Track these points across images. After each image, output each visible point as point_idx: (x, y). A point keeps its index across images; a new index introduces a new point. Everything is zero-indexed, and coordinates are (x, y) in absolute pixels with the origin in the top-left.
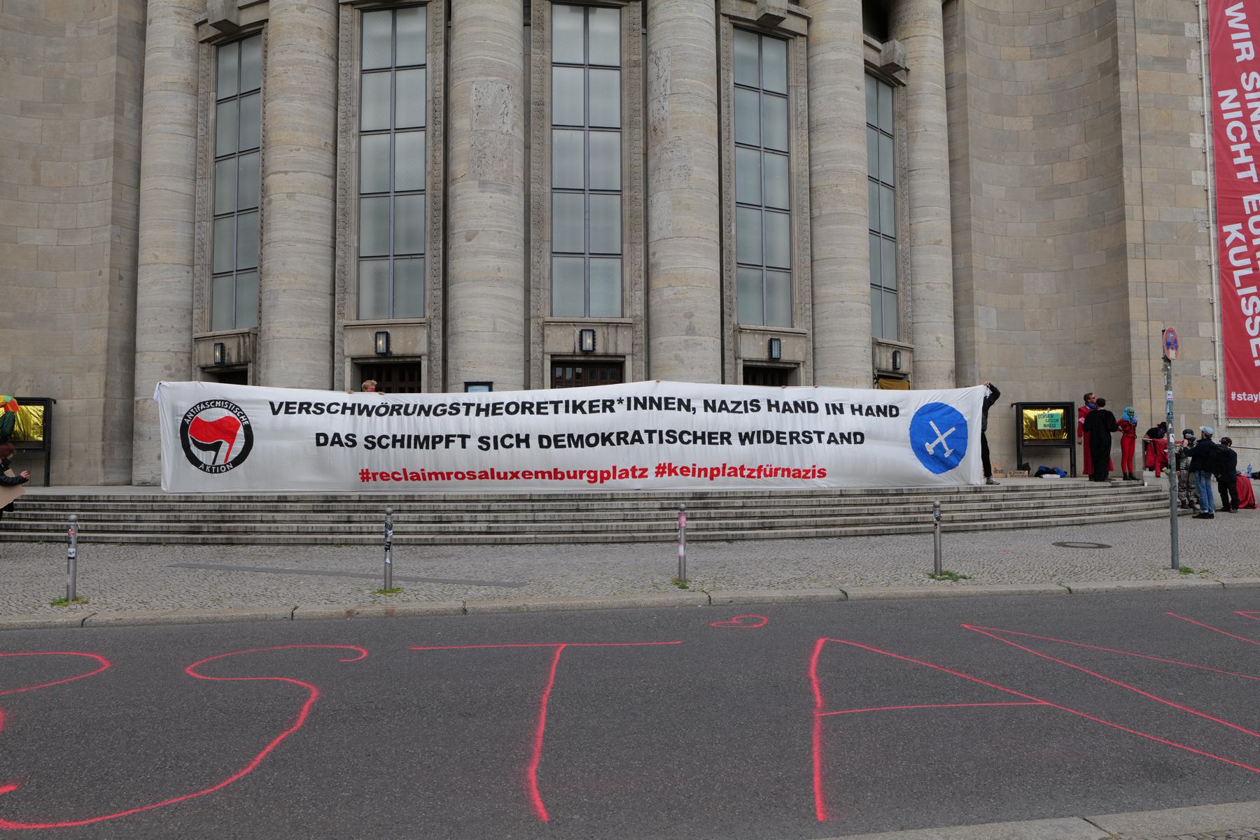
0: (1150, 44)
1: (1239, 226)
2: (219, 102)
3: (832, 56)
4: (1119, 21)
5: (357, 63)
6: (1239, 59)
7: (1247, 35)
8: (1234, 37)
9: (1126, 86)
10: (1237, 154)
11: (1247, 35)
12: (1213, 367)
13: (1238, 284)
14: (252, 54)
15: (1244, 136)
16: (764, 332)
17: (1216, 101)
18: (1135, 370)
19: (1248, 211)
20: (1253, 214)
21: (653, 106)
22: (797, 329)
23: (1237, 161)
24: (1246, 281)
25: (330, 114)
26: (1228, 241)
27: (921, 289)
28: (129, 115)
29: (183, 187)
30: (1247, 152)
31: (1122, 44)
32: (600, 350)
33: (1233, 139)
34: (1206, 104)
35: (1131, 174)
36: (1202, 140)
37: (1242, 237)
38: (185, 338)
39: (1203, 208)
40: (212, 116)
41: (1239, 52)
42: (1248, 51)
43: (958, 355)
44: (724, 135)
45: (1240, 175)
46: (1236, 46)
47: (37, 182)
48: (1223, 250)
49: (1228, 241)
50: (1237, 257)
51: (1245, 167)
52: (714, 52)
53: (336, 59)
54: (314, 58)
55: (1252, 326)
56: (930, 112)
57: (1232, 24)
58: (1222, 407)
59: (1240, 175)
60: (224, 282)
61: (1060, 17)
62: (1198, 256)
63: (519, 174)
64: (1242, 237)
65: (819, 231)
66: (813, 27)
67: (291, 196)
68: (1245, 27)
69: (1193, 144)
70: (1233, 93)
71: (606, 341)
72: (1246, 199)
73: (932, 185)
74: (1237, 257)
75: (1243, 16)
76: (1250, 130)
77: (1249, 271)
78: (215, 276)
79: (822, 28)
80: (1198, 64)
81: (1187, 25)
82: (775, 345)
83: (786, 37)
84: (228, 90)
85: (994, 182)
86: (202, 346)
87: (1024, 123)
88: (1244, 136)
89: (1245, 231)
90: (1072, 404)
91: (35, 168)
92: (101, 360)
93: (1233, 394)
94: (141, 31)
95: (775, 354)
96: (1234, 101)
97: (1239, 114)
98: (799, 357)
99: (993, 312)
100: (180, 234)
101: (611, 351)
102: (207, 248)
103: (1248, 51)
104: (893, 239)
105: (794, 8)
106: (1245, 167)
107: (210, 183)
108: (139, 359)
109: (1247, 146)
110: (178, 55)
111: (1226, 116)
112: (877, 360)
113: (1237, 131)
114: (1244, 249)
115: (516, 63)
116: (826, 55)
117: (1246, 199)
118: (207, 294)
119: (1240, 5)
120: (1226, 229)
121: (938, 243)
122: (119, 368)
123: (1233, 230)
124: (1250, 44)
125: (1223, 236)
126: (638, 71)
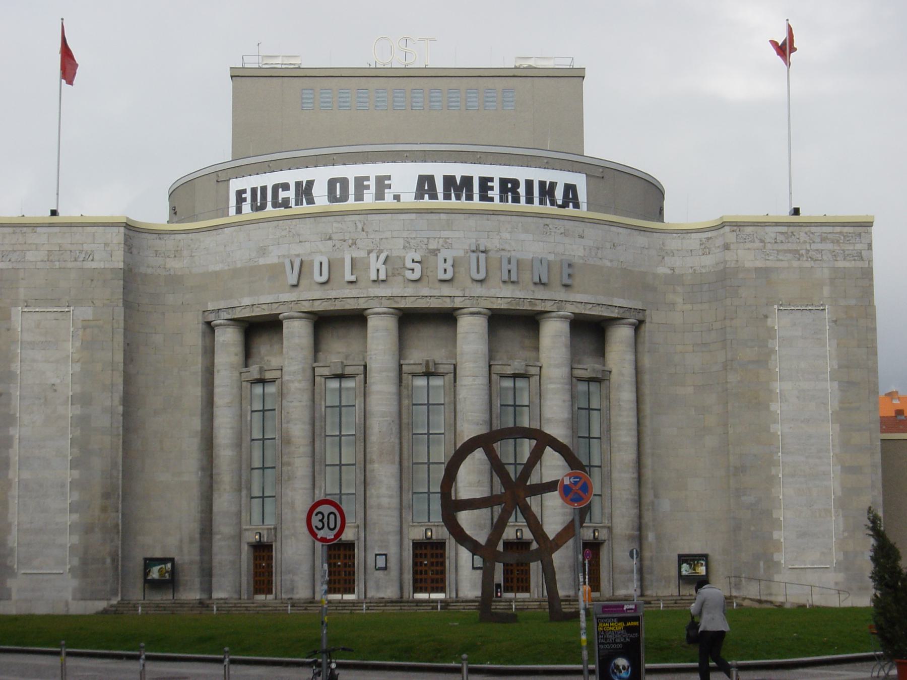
2: (252, 411)
5: (323, 403)
14: (271, 389)
32: (434, 537)
53: (313, 400)
62: (773, 472)
63: (397, 459)
66: (543, 370)
71: (437, 532)
84: (258, 406)
87: (690, 390)
90: (680, 556)
94: (209, 372)
101: (440, 537)
115: (394, 408)
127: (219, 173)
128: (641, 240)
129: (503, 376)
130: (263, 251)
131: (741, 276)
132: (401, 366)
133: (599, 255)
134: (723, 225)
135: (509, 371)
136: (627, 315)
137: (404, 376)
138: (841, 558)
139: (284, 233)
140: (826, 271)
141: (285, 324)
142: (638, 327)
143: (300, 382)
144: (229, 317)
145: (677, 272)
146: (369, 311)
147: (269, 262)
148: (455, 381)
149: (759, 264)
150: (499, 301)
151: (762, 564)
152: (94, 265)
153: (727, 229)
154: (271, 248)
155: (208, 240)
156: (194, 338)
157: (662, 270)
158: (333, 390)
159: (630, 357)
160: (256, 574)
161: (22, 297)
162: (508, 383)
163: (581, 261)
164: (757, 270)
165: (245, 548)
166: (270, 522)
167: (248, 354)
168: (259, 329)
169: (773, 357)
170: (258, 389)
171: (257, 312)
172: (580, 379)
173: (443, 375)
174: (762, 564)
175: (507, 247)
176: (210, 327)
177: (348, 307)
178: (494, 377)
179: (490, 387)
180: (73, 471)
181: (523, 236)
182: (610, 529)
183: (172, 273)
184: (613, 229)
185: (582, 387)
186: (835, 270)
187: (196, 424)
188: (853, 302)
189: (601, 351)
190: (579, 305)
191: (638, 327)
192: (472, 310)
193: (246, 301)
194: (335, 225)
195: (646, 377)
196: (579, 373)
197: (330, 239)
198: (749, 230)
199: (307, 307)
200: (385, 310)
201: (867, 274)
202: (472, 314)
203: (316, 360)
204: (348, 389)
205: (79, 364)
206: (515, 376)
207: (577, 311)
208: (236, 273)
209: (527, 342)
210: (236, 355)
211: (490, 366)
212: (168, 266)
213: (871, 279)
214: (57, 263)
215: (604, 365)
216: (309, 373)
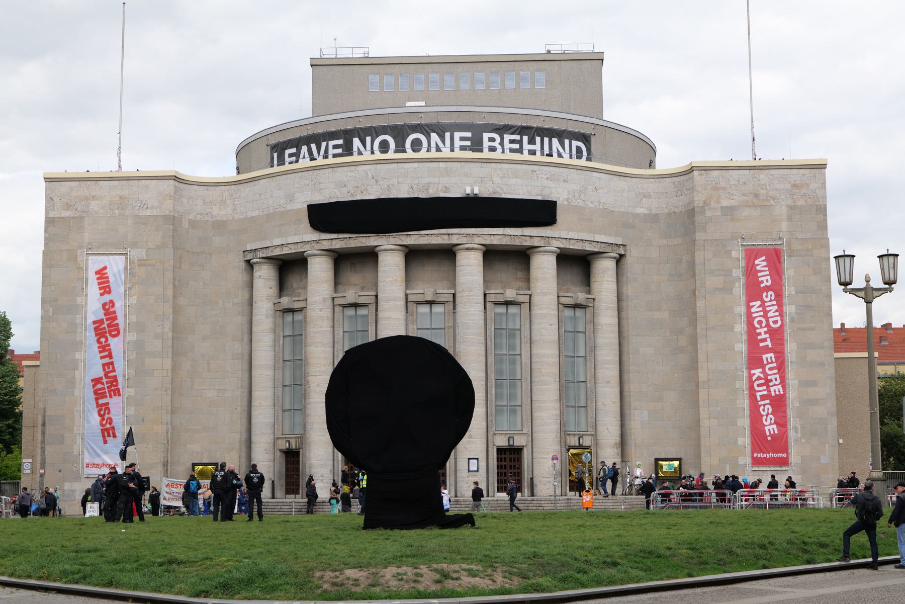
0: (713, 281)
1: (760, 370)
3: (539, 312)
4: (697, 271)
6: (762, 285)
7: (767, 273)
8: (759, 274)
9: (700, 304)
10: (760, 334)
11: (767, 273)
12: (745, 441)
13: (759, 399)
14: (298, 317)
15: (764, 325)
16: (506, 434)
17: (749, 308)
18: (702, 443)
19: (765, 362)
20: (768, 363)
21: (457, 345)
22: (524, 432)
23: (759, 337)
24: (763, 398)
25: (331, 350)
26: (754, 378)
27: (599, 405)
28: (246, 340)
29: (270, 373)
30: (766, 333)
31: (698, 282)
33: (758, 326)
34: (742, 309)
35: (702, 347)
36: (741, 328)
37: (762, 376)
38: (272, 436)
39: (742, 361)
40: (281, 342)
41: (762, 282)
42: (767, 281)
43: (623, 436)
44: (489, 352)
45: (761, 344)
46: (760, 279)
47: (209, 370)
48: (751, 383)
49: (754, 378)
50: (759, 385)
51: (764, 340)
52: (482, 322)
54: (325, 329)
55: (766, 420)
56: (607, 318)
57: (758, 268)
58: (748, 460)
59: (761, 344)
60: (287, 413)
61: (681, 261)
62: (738, 386)
64: (762, 376)
65: (534, 388)
67: (318, 385)
68: (766, 269)
69: (736, 330)
70: (758, 303)
72: (764, 356)
73: (607, 355)
74: (759, 385)
75: (765, 263)
76: (767, 321)
77: (766, 392)
78: (284, 411)
79: (535, 299)
80: (739, 289)
81: (734, 270)
82: (511, 440)
83: (519, 304)
84: (288, 332)
85: (643, 347)
86: (280, 441)
87: (664, 315)
88: (764, 325)
89: (764, 372)
91: (208, 364)
92: (237, 446)
93: (755, 455)
94: (251, 302)
95: (511, 443)
96: (759, 307)
97: (762, 313)
98: (524, 443)
99: (646, 413)
100: (269, 393)
102: (280, 399)
103: (767, 281)
104: (585, 382)
105: (521, 292)
106: (764, 340)
107: (281, 371)
108: (253, 446)
109: (766, 329)
110: (267, 317)
111: (754, 315)
112: (568, 442)
113: (760, 322)
114: (763, 381)
116: (536, 311)
117: (764, 356)
118: (280, 418)
119: (764, 258)
120: (752, 372)
121: (608, 382)
122: (244, 449)
123: (757, 372)
124: (768, 278)
125: (751, 376)
126: (451, 330)
127: (269, 137)
128: (621, 183)
129: (496, 304)
130: (291, 198)
131: (708, 213)
132: (407, 295)
133: (582, 197)
134: (691, 170)
135: (501, 299)
136: (608, 249)
137: (410, 304)
138: (799, 462)
139: (307, 182)
140: (784, 209)
141: (310, 260)
142: (620, 260)
143: (321, 310)
144: (265, 255)
145: (654, 212)
146: (378, 248)
147: (295, 208)
148: (454, 308)
149: (725, 203)
150: (493, 237)
151: (728, 466)
152: (148, 213)
153: (696, 173)
154: (297, 195)
155: (246, 189)
156: (238, 274)
157: (641, 210)
158: (350, 317)
159: (613, 286)
160: (287, 476)
161: (87, 240)
162: (501, 310)
163: (566, 203)
164: (724, 209)
165: (278, 453)
166: (298, 430)
167: (282, 287)
168: (290, 267)
169: (737, 285)
170: (289, 317)
171: (286, 251)
172: (566, 306)
173: (443, 303)
174: (728, 466)
175: (498, 190)
176: (250, 265)
177: (359, 245)
178: (488, 304)
179: (485, 313)
180: (130, 390)
181: (513, 181)
182: (595, 437)
183: (218, 219)
184: (595, 174)
185: (568, 313)
186: (791, 208)
187: (239, 348)
188: (808, 235)
189: (587, 280)
190: (564, 241)
191: (620, 260)
192: (467, 246)
193: (277, 242)
194: (349, 174)
195: (624, 304)
196: (564, 300)
197: (345, 186)
198: (716, 173)
199: (326, 245)
200: (393, 247)
201: (822, 210)
202: (468, 249)
203: (336, 291)
204: (363, 316)
205: (135, 298)
206: (508, 303)
207: (562, 246)
208: (269, 217)
209: (520, 274)
210: (271, 288)
211: (485, 295)
212: (214, 213)
213: (825, 215)
214: (117, 211)
215: (589, 292)
216: (329, 303)
